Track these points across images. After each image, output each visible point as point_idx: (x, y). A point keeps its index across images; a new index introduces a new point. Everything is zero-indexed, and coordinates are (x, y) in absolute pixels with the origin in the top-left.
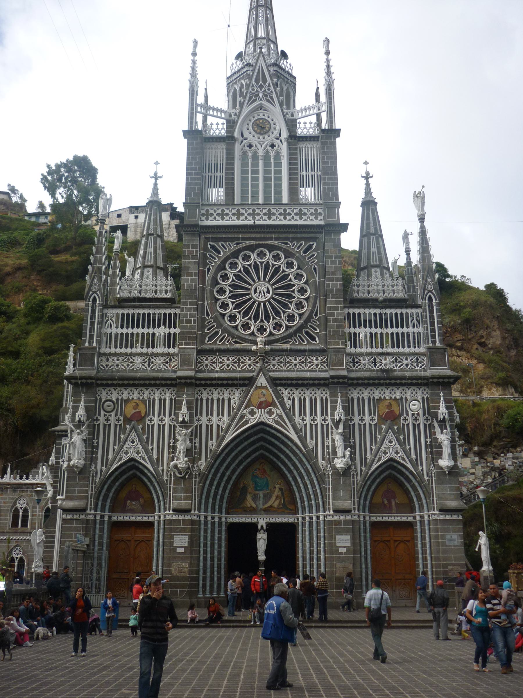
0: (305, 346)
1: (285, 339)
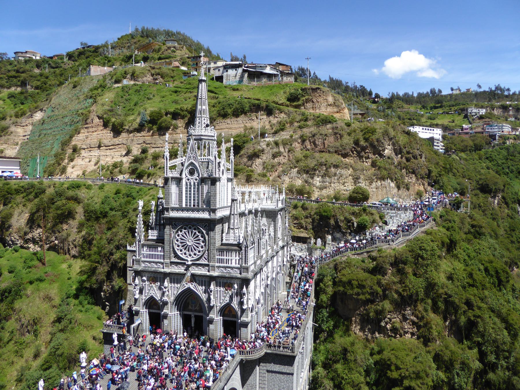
0: (204, 263)
1: (198, 260)
